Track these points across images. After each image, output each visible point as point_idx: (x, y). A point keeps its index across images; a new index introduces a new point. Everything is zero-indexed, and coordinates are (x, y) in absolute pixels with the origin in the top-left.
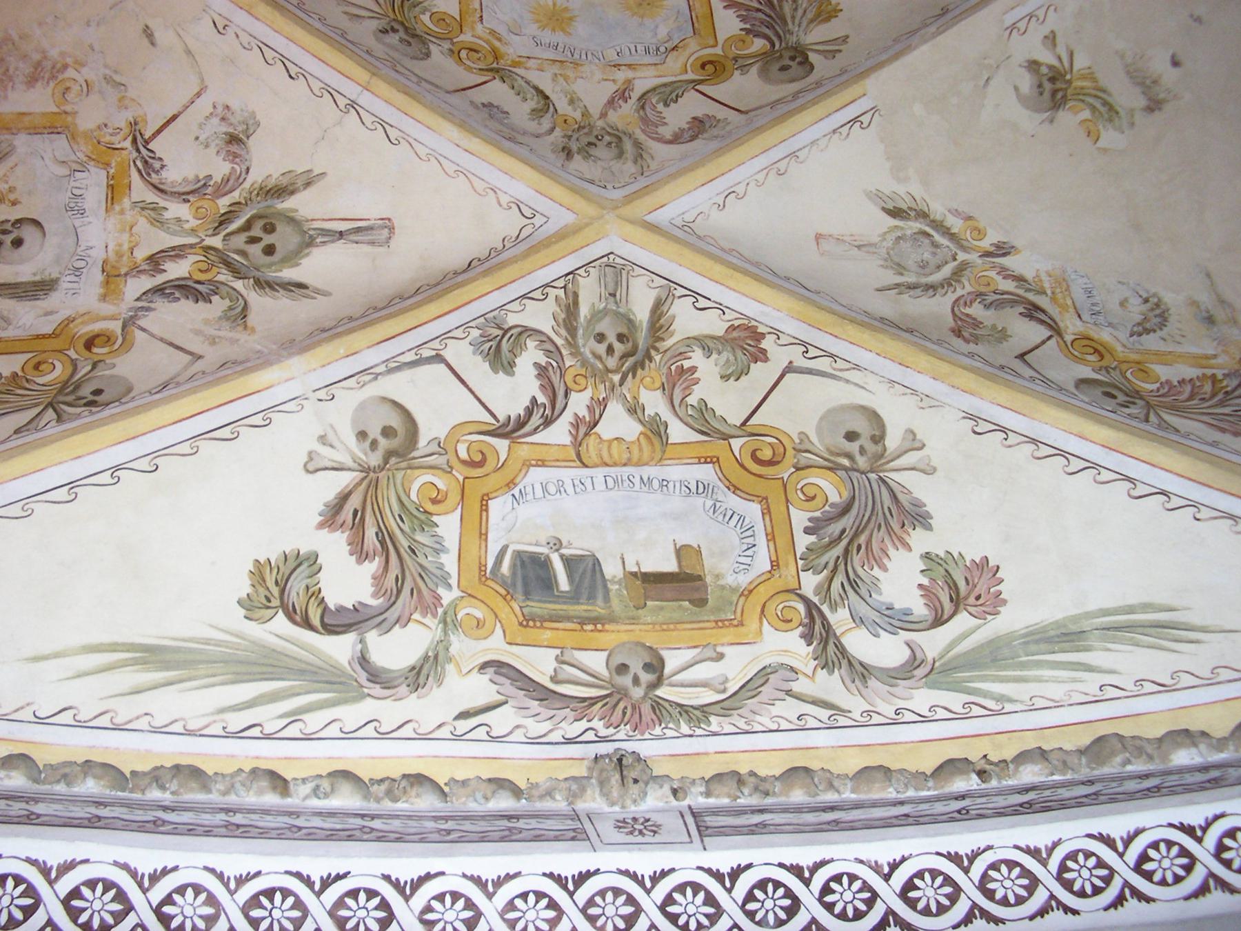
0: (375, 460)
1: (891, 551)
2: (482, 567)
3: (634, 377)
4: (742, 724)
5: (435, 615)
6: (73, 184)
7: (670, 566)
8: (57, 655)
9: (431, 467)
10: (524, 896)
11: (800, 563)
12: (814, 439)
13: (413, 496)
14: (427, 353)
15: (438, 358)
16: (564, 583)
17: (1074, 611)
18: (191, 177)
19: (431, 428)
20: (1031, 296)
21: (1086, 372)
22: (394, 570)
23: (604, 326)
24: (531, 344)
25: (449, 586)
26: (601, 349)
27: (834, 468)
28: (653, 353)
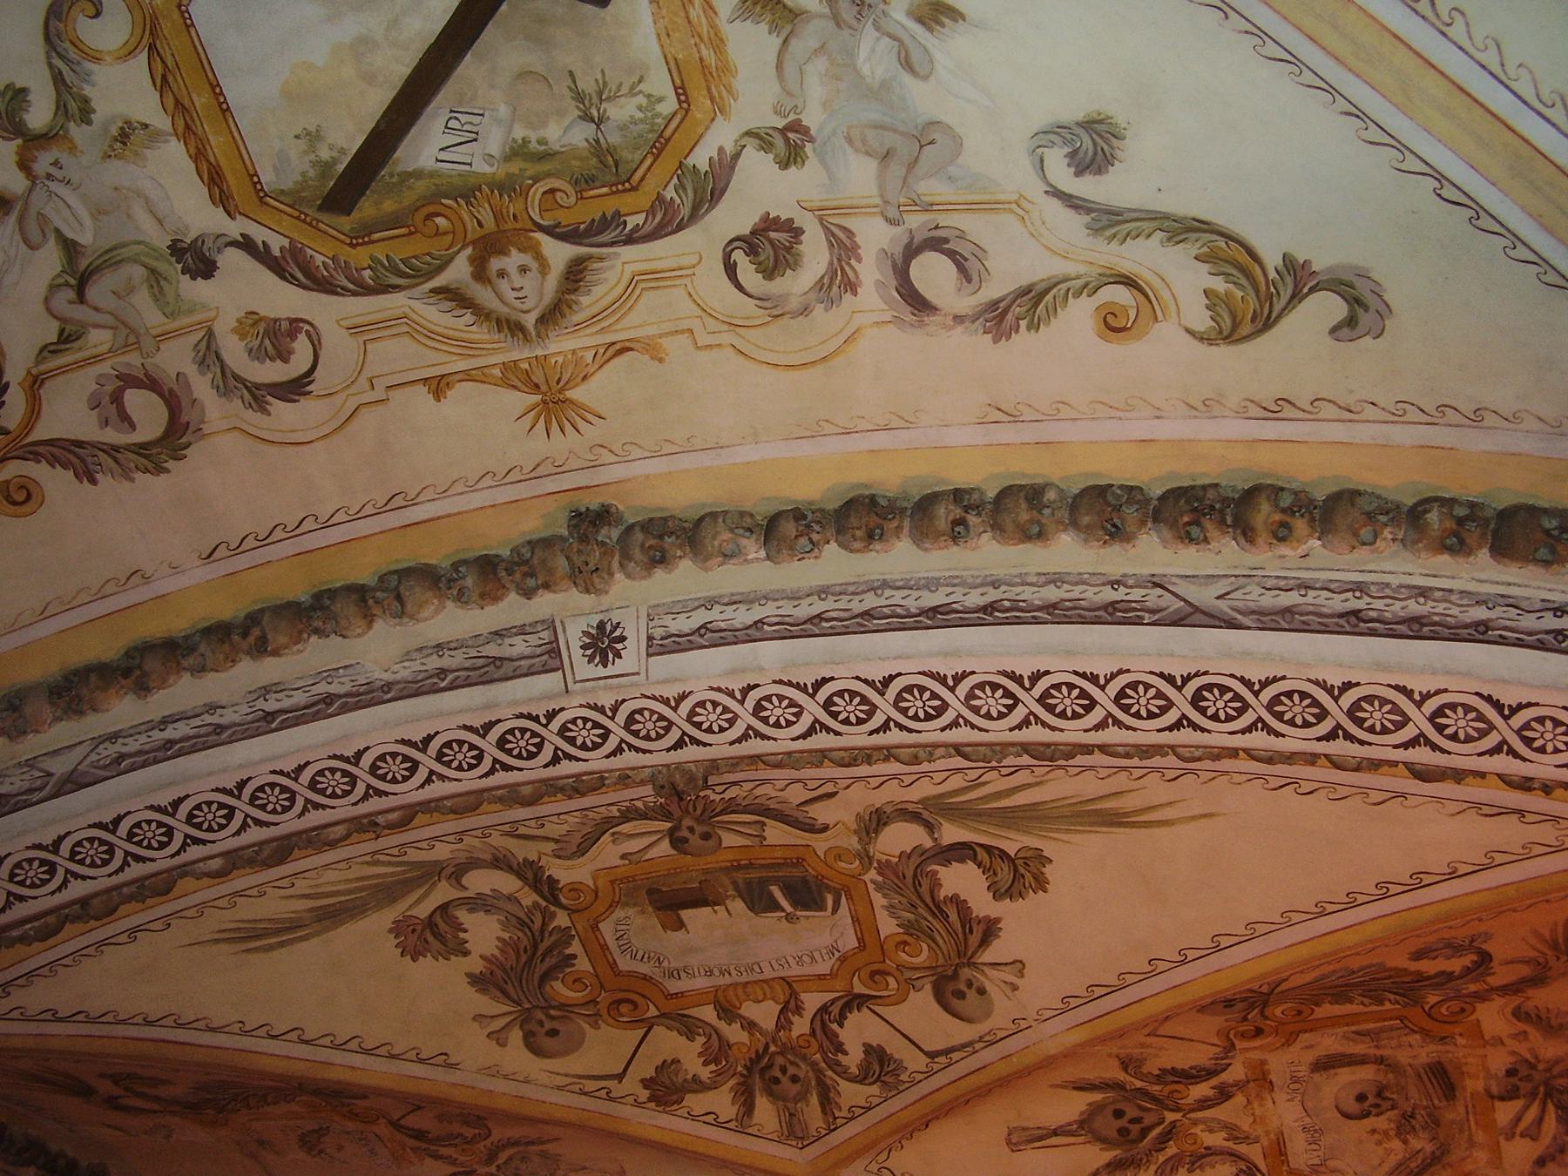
0: (966, 973)
1: (497, 952)
2: (850, 897)
3: (757, 1052)
4: (591, 814)
5: (879, 861)
6: (1320, 1153)
7: (686, 914)
8: (1194, 818)
9: (915, 969)
10: (722, 730)
11: (573, 933)
12: (586, 1026)
13: (925, 946)
14: (942, 1059)
15: (931, 1055)
16: (776, 891)
17: (331, 934)
18: (1208, 1170)
19: (923, 998)
20: (424, 1146)
21: (359, 1102)
22: (924, 890)
23: (796, 1088)
24: (854, 1070)
25: (873, 882)
26: (791, 1070)
27: (562, 1007)
28: (745, 1072)
